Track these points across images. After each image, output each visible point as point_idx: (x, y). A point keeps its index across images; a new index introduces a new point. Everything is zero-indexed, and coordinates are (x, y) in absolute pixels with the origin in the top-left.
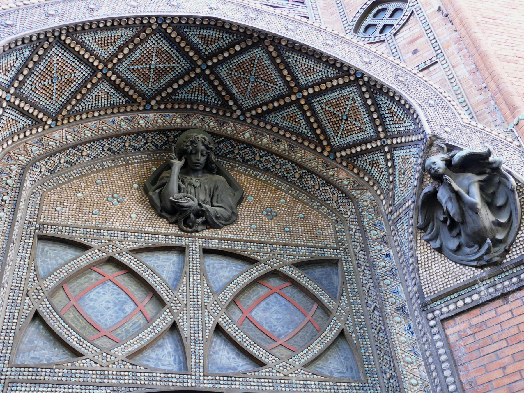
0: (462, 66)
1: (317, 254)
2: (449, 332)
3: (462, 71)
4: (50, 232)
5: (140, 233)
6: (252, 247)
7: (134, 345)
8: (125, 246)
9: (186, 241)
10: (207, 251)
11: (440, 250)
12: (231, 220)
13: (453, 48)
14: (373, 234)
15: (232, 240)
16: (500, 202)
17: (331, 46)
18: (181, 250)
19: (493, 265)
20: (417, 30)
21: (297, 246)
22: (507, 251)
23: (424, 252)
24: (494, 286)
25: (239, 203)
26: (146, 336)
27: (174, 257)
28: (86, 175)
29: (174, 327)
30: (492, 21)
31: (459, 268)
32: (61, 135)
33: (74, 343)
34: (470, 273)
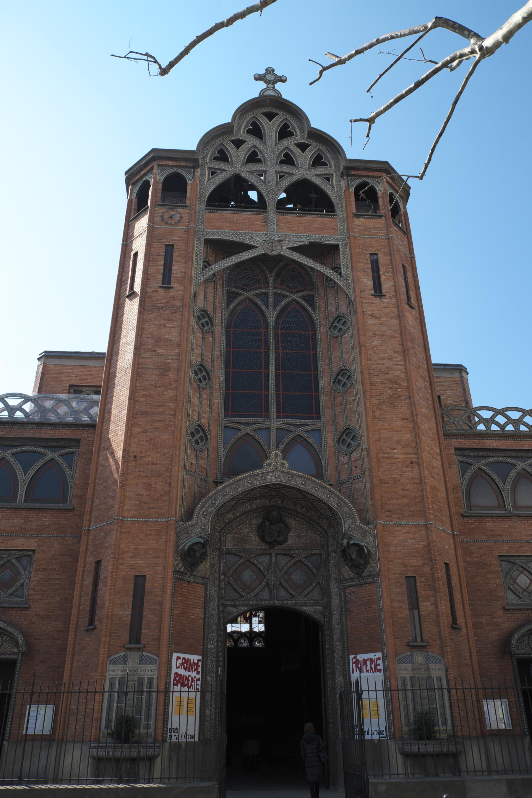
0: (368, 484)
1: (314, 552)
2: (346, 591)
3: (368, 486)
4: (229, 551)
5: (257, 549)
6: (292, 552)
7: (256, 591)
8: (253, 555)
9: (271, 551)
10: (277, 554)
11: (347, 564)
12: (285, 541)
13: (367, 473)
14: (331, 548)
15: (286, 549)
16: (363, 556)
17: (317, 491)
18: (270, 554)
19: (359, 575)
20: (358, 455)
21: (307, 549)
22: (363, 572)
23: (342, 564)
24: (359, 581)
25: (288, 533)
26: (259, 588)
27: (268, 557)
28: (239, 526)
29: (268, 584)
30: (386, 456)
31: (351, 572)
32: (230, 516)
33: (240, 591)
34: (353, 575)
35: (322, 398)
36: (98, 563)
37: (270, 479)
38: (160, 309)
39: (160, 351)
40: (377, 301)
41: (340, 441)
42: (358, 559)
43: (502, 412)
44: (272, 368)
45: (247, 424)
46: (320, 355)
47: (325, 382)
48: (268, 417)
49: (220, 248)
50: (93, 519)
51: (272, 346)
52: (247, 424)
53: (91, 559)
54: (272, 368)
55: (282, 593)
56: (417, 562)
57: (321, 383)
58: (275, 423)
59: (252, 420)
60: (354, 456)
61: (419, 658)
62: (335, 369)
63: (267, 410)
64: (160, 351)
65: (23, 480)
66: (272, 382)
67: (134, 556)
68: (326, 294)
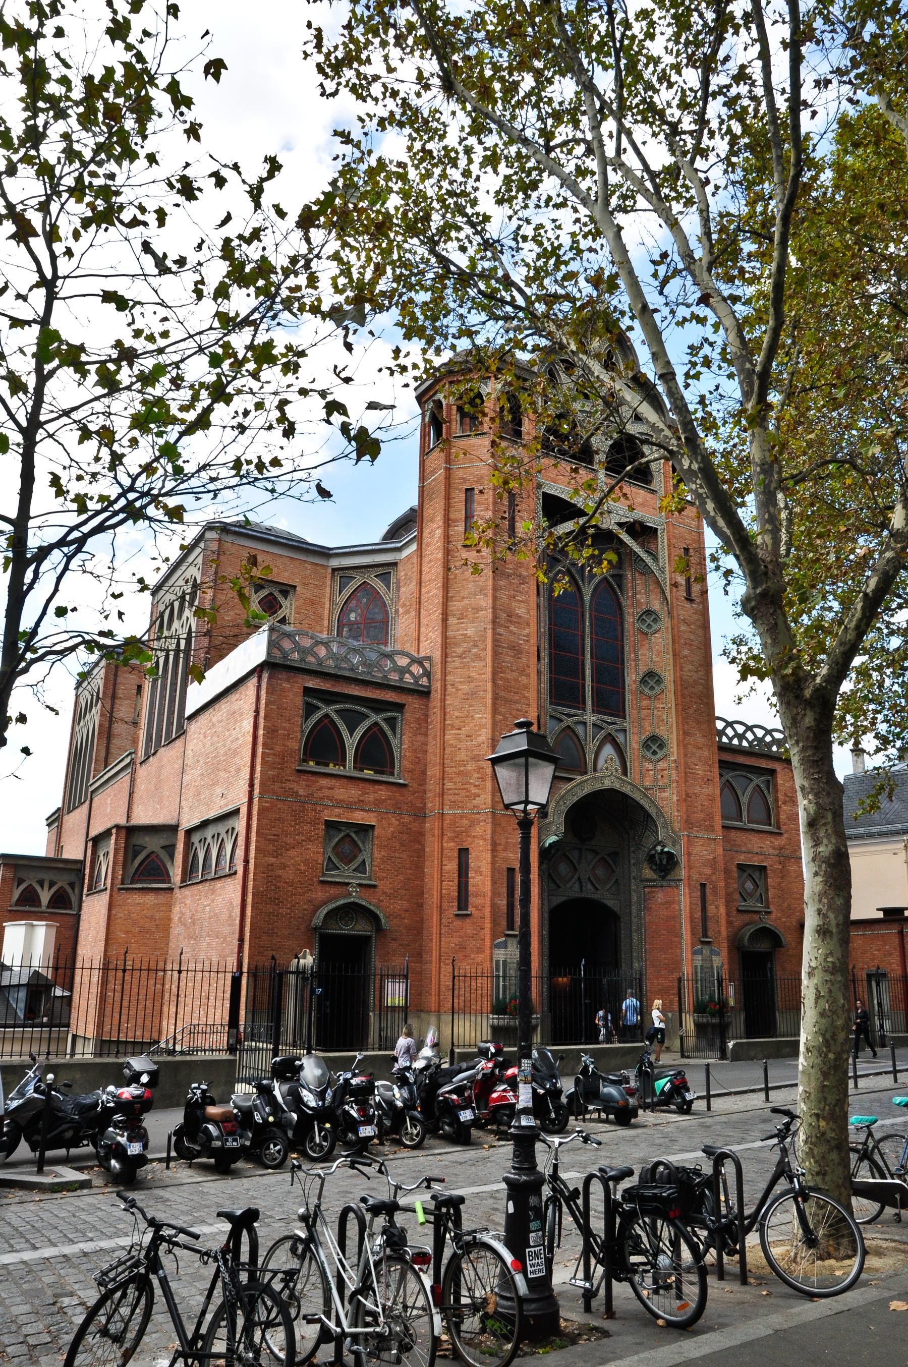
23: (645, 865)
35: (628, 697)
36: (463, 853)
37: (607, 784)
38: (509, 575)
39: (512, 628)
40: (687, 605)
41: (646, 745)
42: (666, 865)
43: (749, 728)
44: (588, 656)
45: (569, 716)
46: (626, 649)
47: (631, 678)
48: (584, 709)
49: (556, 509)
50: (446, 802)
51: (588, 630)
52: (569, 716)
53: (451, 847)
54: (588, 656)
55: (589, 886)
56: (708, 871)
57: (628, 681)
58: (591, 718)
59: (572, 711)
60: (661, 765)
61: (706, 951)
62: (643, 669)
63: (584, 703)
64: (512, 628)
65: (351, 742)
66: (588, 672)
67: (505, 850)
68: (634, 579)
